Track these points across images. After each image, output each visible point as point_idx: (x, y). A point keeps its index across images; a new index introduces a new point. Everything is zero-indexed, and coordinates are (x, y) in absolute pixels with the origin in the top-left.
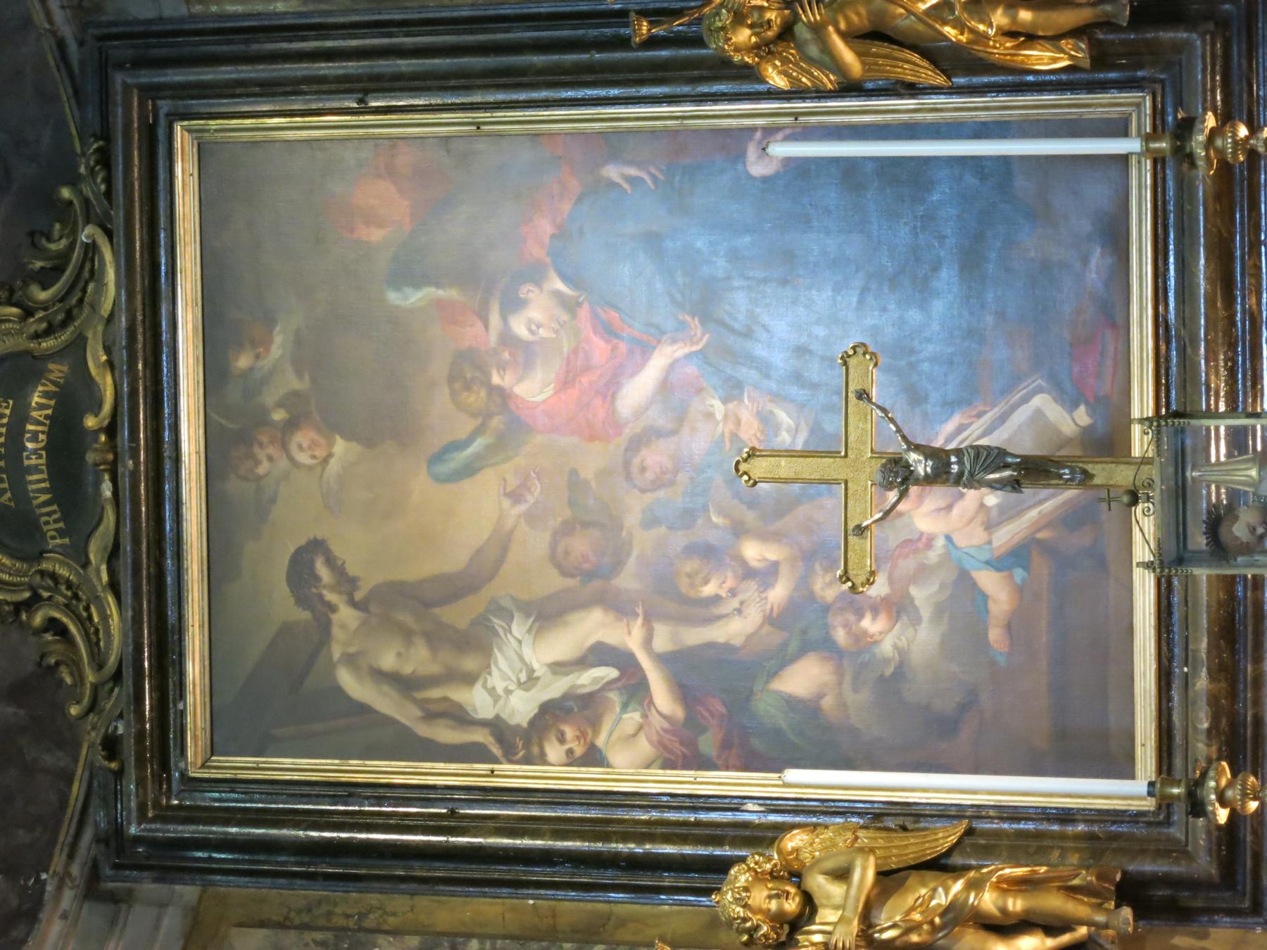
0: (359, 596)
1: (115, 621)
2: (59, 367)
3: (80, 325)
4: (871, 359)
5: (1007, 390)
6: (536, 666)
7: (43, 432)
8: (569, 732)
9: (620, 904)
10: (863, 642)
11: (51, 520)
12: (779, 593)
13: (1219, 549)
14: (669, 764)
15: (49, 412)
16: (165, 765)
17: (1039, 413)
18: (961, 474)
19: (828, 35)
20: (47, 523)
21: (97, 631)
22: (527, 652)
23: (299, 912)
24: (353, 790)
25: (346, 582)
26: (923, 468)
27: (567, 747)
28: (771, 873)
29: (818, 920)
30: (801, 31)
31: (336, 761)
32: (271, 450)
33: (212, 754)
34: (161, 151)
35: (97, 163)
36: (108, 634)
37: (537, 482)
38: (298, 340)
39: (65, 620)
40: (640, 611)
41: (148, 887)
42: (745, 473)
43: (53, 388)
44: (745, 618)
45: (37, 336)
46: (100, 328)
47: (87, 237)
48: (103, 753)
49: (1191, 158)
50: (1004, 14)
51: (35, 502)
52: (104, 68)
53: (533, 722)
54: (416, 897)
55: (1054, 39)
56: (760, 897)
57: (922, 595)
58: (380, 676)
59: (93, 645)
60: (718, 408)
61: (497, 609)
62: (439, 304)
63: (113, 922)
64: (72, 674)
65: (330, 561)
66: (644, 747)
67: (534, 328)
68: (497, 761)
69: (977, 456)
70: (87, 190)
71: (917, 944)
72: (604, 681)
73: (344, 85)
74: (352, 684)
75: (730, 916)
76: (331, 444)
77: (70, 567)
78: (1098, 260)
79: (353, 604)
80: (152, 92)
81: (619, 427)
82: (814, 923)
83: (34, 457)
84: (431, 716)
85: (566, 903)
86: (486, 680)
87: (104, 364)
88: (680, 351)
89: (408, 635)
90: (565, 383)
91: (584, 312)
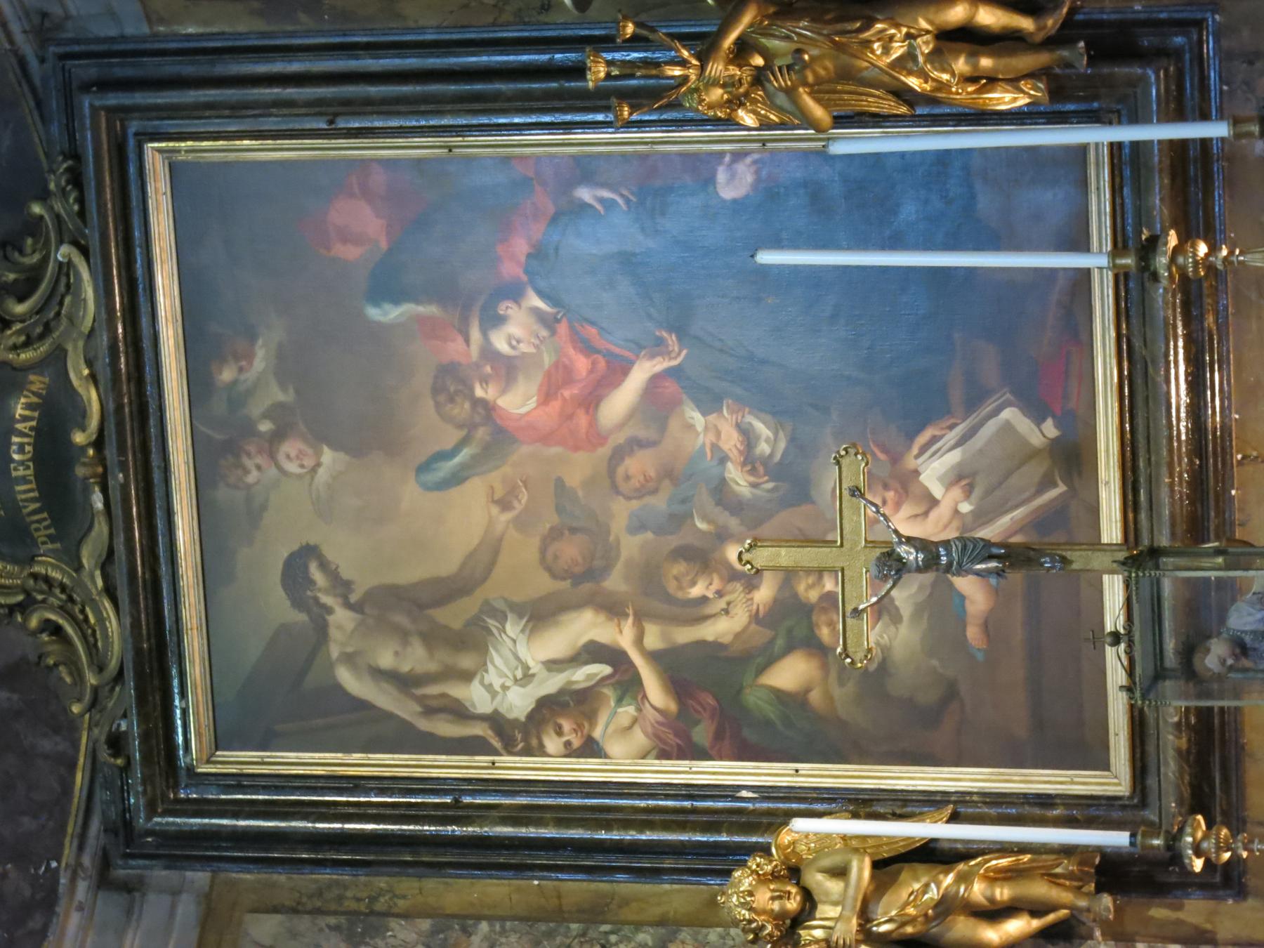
0: (353, 598)
1: (113, 625)
2: (41, 378)
3: (58, 337)
4: (863, 459)
6: (531, 663)
7: (29, 444)
8: (567, 725)
9: (625, 886)
12: (764, 594)
14: (664, 755)
15: (34, 423)
17: (1008, 427)
18: (950, 564)
19: (799, 96)
20: (37, 530)
21: (94, 632)
22: (523, 651)
23: (311, 897)
24: (356, 782)
25: (342, 586)
27: (565, 739)
28: (772, 874)
29: (818, 915)
31: (340, 755)
32: (259, 460)
33: (217, 749)
34: (132, 170)
35: (68, 182)
36: (106, 636)
37: (524, 490)
39: (61, 621)
40: (631, 612)
41: (159, 874)
42: (748, 562)
43: (35, 400)
44: (732, 617)
45: (15, 348)
46: (81, 344)
47: (64, 256)
48: (108, 751)
49: (1155, 277)
50: (966, 62)
51: (25, 511)
53: (530, 716)
54: (423, 879)
55: (1013, 82)
56: (763, 898)
58: (379, 674)
59: (91, 648)
60: (697, 418)
61: (490, 610)
62: (421, 320)
63: (129, 912)
64: (71, 674)
65: (324, 565)
66: (639, 738)
67: (514, 343)
68: (497, 753)
69: (965, 547)
70: (58, 207)
71: (911, 934)
72: (599, 677)
73: (317, 106)
75: (736, 918)
76: (318, 454)
77: (63, 572)
79: (348, 605)
82: (814, 919)
83: (21, 468)
84: (430, 711)
85: (570, 883)
86: (483, 677)
87: (86, 377)
88: (659, 365)
90: (547, 396)
91: (563, 329)
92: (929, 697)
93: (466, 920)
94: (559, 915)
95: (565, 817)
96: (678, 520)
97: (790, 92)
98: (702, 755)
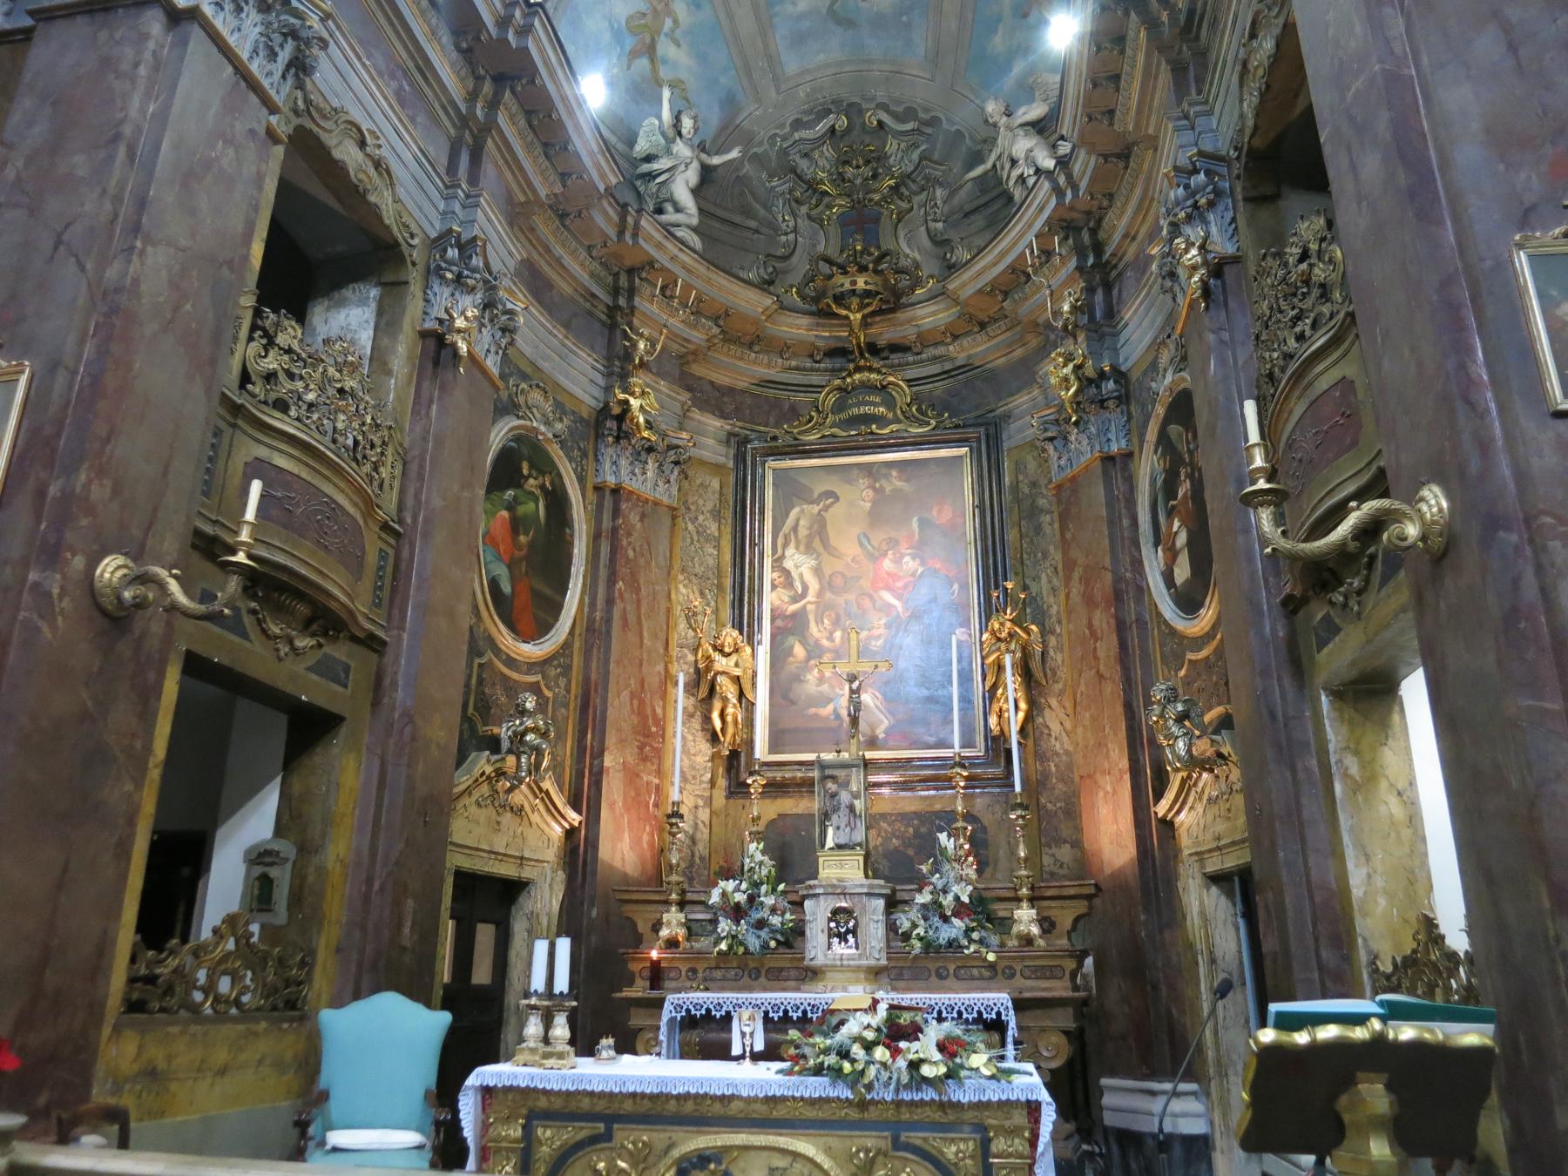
5: (890, 713)
9: (729, 597)
10: (810, 670)
11: (843, 416)
12: (825, 643)
13: (824, 778)
14: (772, 610)
25: (826, 508)
26: (855, 685)
38: (901, 490)
41: (732, 452)
49: (953, 767)
52: (986, 424)
56: (729, 640)
57: (825, 688)
58: (798, 521)
59: (805, 431)
60: (883, 622)
65: (832, 503)
66: (777, 603)
73: (982, 501)
78: (932, 740)
80: (979, 440)
81: (876, 591)
84: (786, 537)
88: (900, 609)
90: (889, 574)
92: (792, 695)
93: (718, 547)
94: (720, 576)
95: (752, 578)
96: (849, 615)
97: (999, 649)
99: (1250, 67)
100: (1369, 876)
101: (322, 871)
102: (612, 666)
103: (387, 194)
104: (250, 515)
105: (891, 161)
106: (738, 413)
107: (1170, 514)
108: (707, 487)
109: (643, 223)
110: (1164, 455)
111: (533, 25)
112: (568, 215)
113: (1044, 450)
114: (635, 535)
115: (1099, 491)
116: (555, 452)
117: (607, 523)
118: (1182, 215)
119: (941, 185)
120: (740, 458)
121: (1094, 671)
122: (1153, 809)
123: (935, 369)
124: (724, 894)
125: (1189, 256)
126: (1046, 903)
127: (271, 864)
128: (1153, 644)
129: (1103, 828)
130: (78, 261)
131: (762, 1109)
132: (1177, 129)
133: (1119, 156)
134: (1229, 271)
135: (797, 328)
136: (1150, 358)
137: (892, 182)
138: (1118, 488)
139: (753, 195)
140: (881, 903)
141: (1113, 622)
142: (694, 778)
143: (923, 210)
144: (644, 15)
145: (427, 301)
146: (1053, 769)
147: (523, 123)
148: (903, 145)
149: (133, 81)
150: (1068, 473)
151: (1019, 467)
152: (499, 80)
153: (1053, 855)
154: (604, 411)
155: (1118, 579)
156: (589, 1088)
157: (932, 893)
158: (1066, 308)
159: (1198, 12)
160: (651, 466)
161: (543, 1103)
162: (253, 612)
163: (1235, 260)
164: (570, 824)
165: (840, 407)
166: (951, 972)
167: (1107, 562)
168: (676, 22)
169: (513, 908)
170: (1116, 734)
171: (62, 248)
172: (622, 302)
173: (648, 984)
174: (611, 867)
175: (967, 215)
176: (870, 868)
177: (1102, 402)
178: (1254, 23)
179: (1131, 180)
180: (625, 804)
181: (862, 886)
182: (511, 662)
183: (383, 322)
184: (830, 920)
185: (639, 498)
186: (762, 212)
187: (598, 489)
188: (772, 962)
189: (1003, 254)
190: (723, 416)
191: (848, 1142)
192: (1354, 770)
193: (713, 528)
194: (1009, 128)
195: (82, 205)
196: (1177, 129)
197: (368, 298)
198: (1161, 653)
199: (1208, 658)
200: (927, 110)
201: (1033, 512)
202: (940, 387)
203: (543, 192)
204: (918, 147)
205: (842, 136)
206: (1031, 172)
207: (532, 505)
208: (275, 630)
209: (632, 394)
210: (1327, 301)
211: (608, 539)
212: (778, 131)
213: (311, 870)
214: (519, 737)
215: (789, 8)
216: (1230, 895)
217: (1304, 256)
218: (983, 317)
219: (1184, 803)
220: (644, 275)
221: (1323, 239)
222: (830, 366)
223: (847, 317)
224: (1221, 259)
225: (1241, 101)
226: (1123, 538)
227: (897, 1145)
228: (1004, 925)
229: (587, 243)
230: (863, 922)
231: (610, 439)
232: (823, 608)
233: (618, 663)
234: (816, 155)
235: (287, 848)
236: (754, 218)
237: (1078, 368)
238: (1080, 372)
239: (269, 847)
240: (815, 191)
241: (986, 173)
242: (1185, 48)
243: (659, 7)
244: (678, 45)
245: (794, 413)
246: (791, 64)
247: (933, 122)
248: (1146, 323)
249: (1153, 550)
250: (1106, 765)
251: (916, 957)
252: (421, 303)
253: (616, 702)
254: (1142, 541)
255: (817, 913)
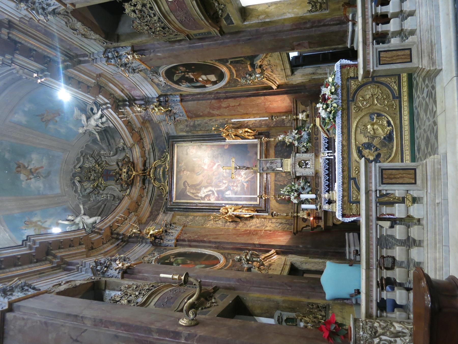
10: (233, 189)
11: (162, 180)
12: (226, 185)
16: (171, 201)
25: (188, 185)
30: (230, 134)
41: (169, 212)
52: (169, 139)
56: (224, 210)
58: (191, 193)
59: (165, 190)
65: (187, 182)
66: (214, 199)
74: (188, 194)
84: (195, 196)
88: (219, 164)
89: (193, 189)
93: (197, 216)
94: (205, 216)
98: (220, 201)
99: (84, 33)
100: (289, 13)
101: (284, 301)
102: (229, 241)
103: (77, 282)
104: (170, 276)
105: (91, 166)
106: (158, 211)
107: (197, 81)
108: (179, 219)
109: (98, 227)
110: (182, 82)
111: (33, 239)
112: (92, 247)
113: (178, 121)
114: (191, 235)
115: (190, 103)
116: (163, 255)
117: (187, 243)
118: (119, 60)
119: (100, 152)
120: (171, 210)
121: (238, 107)
122: (275, 90)
123: (152, 154)
124: (295, 198)
125: (130, 58)
126: (298, 112)
127: (282, 319)
128: (231, 89)
129: (279, 106)
130: (84, 332)
131: (345, 136)
132: (96, 63)
133: (100, 89)
134: (136, 49)
135: (135, 191)
136: (155, 86)
137: (97, 165)
138: (190, 98)
139: (94, 206)
140: (297, 154)
141: (225, 100)
142: (263, 223)
143: (106, 157)
144: (35, 229)
145: (112, 277)
146: (264, 122)
147: (62, 250)
148: (87, 162)
149: (28, 319)
150: (184, 113)
151: (182, 131)
152: (48, 253)
153: (287, 123)
154: (153, 243)
155: (214, 99)
156: (341, 183)
157: (295, 141)
158: (139, 109)
159: (66, 53)
160: (170, 231)
161: (346, 198)
162: (202, 309)
163: (133, 47)
164: (275, 252)
165: (159, 181)
166: (316, 136)
167: (209, 101)
168: (39, 221)
169: (299, 269)
170: (255, 100)
171: (79, 339)
172: (121, 237)
173: (320, 220)
174: (288, 242)
175: (110, 145)
176: (288, 157)
177: (166, 101)
178: (73, 29)
179: (107, 87)
180: (270, 239)
181: (292, 159)
182: (225, 266)
183: (117, 288)
184: (302, 167)
185: (180, 235)
186: (100, 203)
187: (176, 246)
188: (313, 186)
189: (122, 128)
190: (158, 214)
191: (353, 113)
192: (263, 16)
193: (190, 217)
194: (87, 126)
195: (65, 333)
196: (96, 63)
197: (109, 294)
198: (234, 87)
199: (235, 71)
200: (78, 154)
201: (194, 126)
202: (157, 154)
203: (84, 250)
204: (88, 158)
205: (81, 179)
206: (100, 120)
207: (179, 260)
208: (208, 305)
209: (149, 233)
210: (146, 5)
211: (191, 242)
212: (77, 197)
213: (284, 305)
214: (248, 260)
215: (42, 189)
216: (297, 70)
217: (134, 11)
218: (139, 138)
219: (273, 80)
220: (113, 230)
221: (131, 4)
222: (147, 184)
223: (134, 176)
224: (132, 50)
225: (92, 39)
226: (203, 97)
227: (353, 100)
228: (304, 122)
229: (101, 244)
230: (302, 158)
231: (161, 241)
232: (217, 186)
233: (228, 240)
234: (85, 187)
235: (277, 313)
236: (101, 206)
237: (156, 106)
238: (157, 106)
239: (277, 320)
240: (96, 188)
241: (99, 134)
242: (75, 60)
243: (34, 225)
244: (46, 221)
245: (160, 196)
246: (58, 191)
247: (82, 153)
248: (146, 87)
249: (207, 88)
250: (263, 104)
251: (312, 145)
252: (113, 278)
253: (239, 240)
254: (204, 91)
255: (300, 172)
